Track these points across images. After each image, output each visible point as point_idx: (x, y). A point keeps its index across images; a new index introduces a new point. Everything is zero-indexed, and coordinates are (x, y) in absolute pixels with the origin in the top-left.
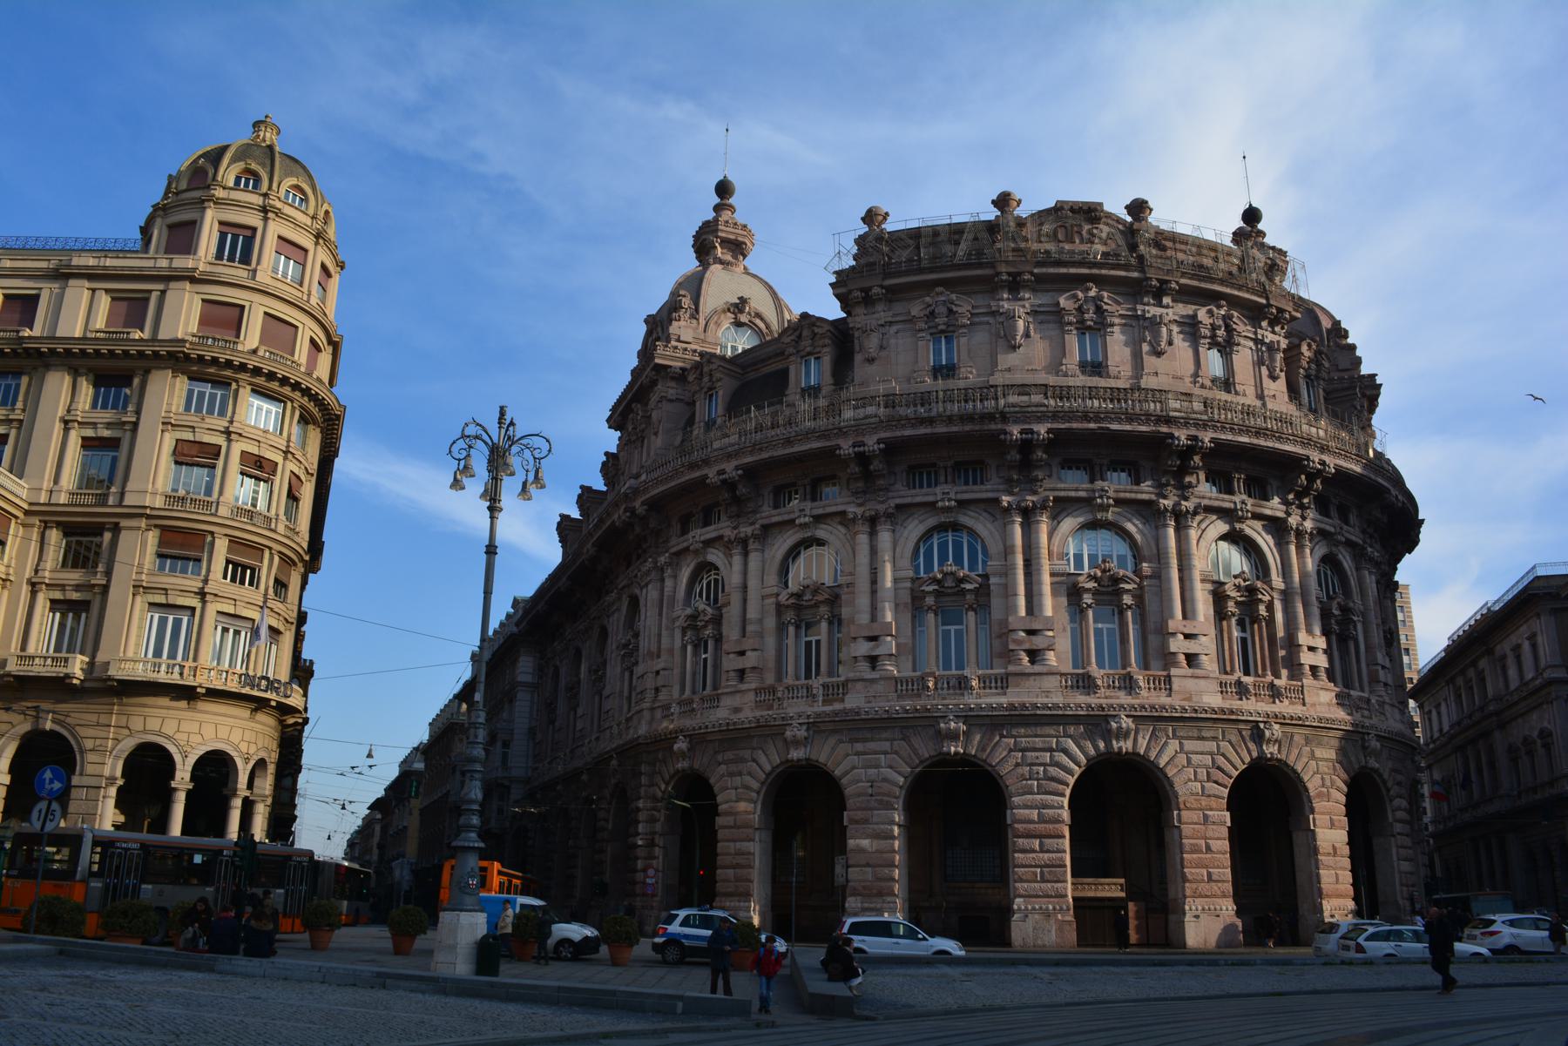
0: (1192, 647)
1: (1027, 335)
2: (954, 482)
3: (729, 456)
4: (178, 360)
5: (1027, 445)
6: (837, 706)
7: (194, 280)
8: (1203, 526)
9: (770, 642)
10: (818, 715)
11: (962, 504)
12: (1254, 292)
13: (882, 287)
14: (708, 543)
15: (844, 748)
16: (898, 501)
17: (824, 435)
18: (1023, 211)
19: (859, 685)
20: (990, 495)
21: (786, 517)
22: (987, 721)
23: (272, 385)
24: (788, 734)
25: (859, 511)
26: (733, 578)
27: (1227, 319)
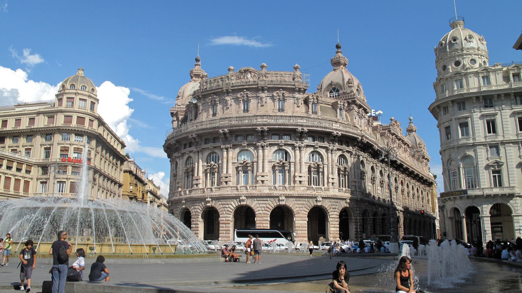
0: (263, 179)
1: (231, 105)
2: (214, 142)
4: (59, 130)
5: (225, 134)
7: (62, 112)
9: (183, 180)
11: (215, 147)
12: (292, 85)
17: (186, 133)
23: (79, 134)
27: (283, 94)
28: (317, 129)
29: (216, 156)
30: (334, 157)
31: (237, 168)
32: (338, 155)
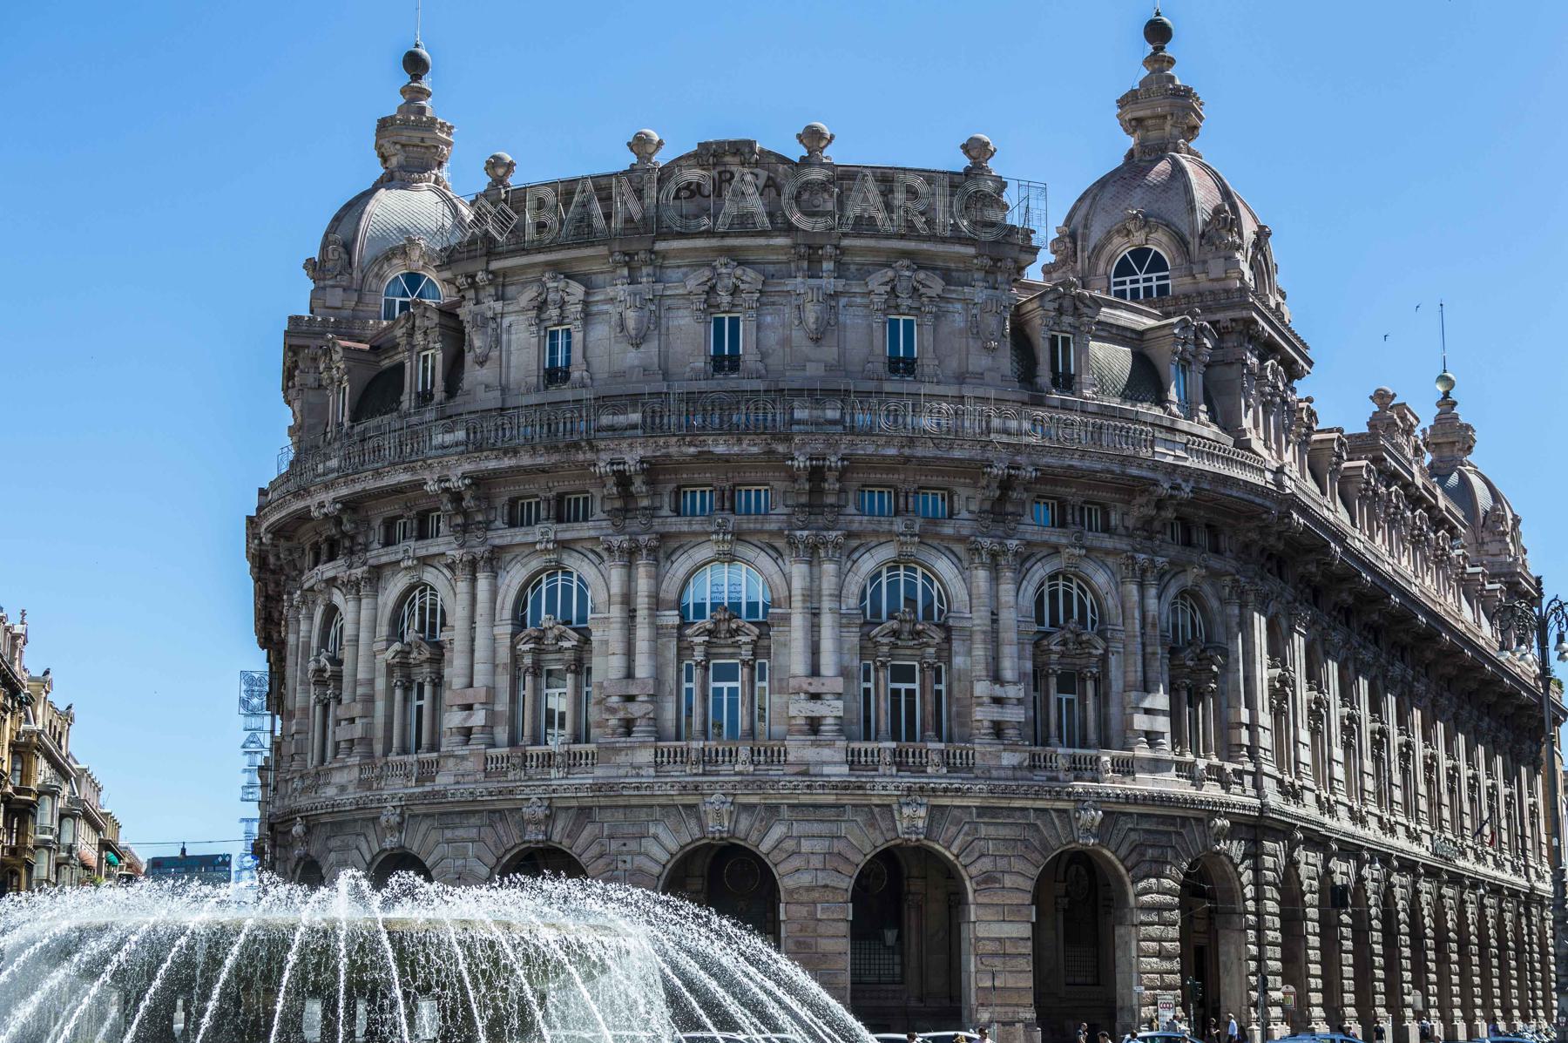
0: (817, 709)
2: (559, 520)
3: (327, 486)
5: (623, 480)
6: (428, 788)
8: (855, 556)
9: (380, 705)
10: (410, 797)
11: (564, 545)
13: (488, 272)
14: (331, 582)
15: (434, 836)
16: (497, 542)
18: (661, 159)
19: (451, 763)
20: (593, 533)
21: (393, 558)
22: (574, 803)
24: (383, 819)
25: (457, 554)
26: (349, 631)
28: (1087, 464)
29: (567, 590)
30: (1152, 604)
31: (684, 650)
32: (1172, 590)
